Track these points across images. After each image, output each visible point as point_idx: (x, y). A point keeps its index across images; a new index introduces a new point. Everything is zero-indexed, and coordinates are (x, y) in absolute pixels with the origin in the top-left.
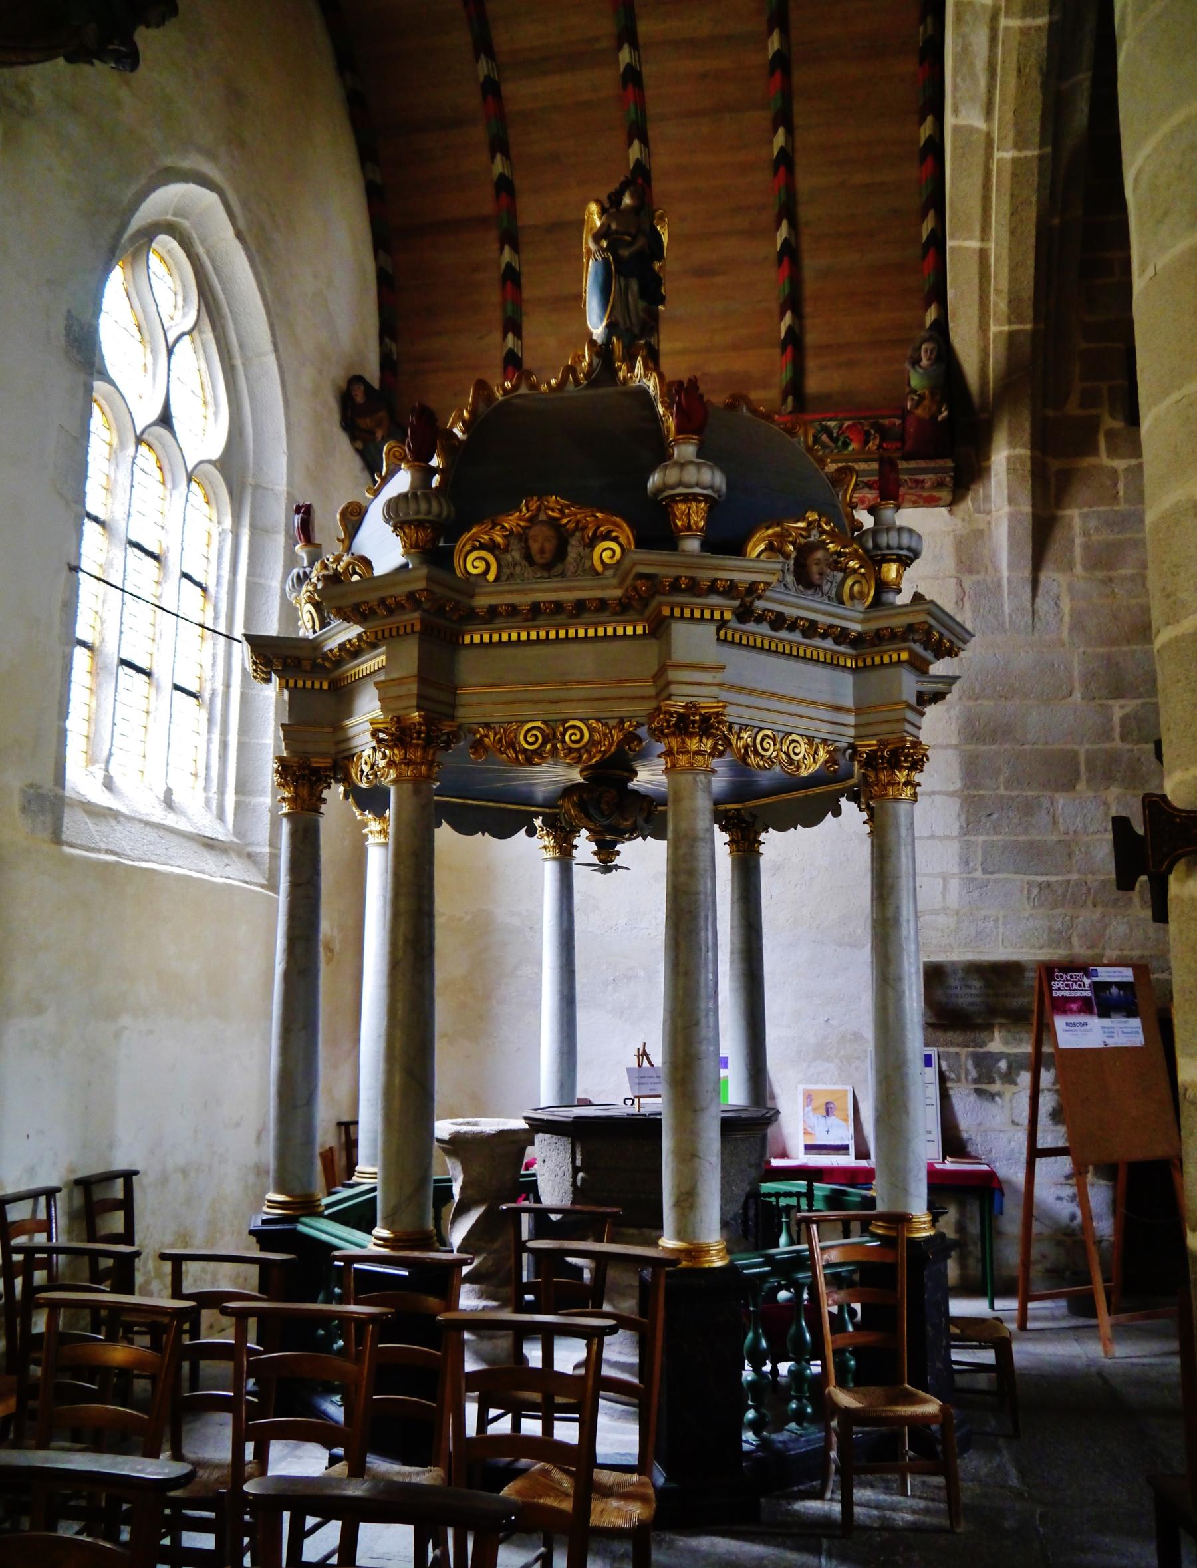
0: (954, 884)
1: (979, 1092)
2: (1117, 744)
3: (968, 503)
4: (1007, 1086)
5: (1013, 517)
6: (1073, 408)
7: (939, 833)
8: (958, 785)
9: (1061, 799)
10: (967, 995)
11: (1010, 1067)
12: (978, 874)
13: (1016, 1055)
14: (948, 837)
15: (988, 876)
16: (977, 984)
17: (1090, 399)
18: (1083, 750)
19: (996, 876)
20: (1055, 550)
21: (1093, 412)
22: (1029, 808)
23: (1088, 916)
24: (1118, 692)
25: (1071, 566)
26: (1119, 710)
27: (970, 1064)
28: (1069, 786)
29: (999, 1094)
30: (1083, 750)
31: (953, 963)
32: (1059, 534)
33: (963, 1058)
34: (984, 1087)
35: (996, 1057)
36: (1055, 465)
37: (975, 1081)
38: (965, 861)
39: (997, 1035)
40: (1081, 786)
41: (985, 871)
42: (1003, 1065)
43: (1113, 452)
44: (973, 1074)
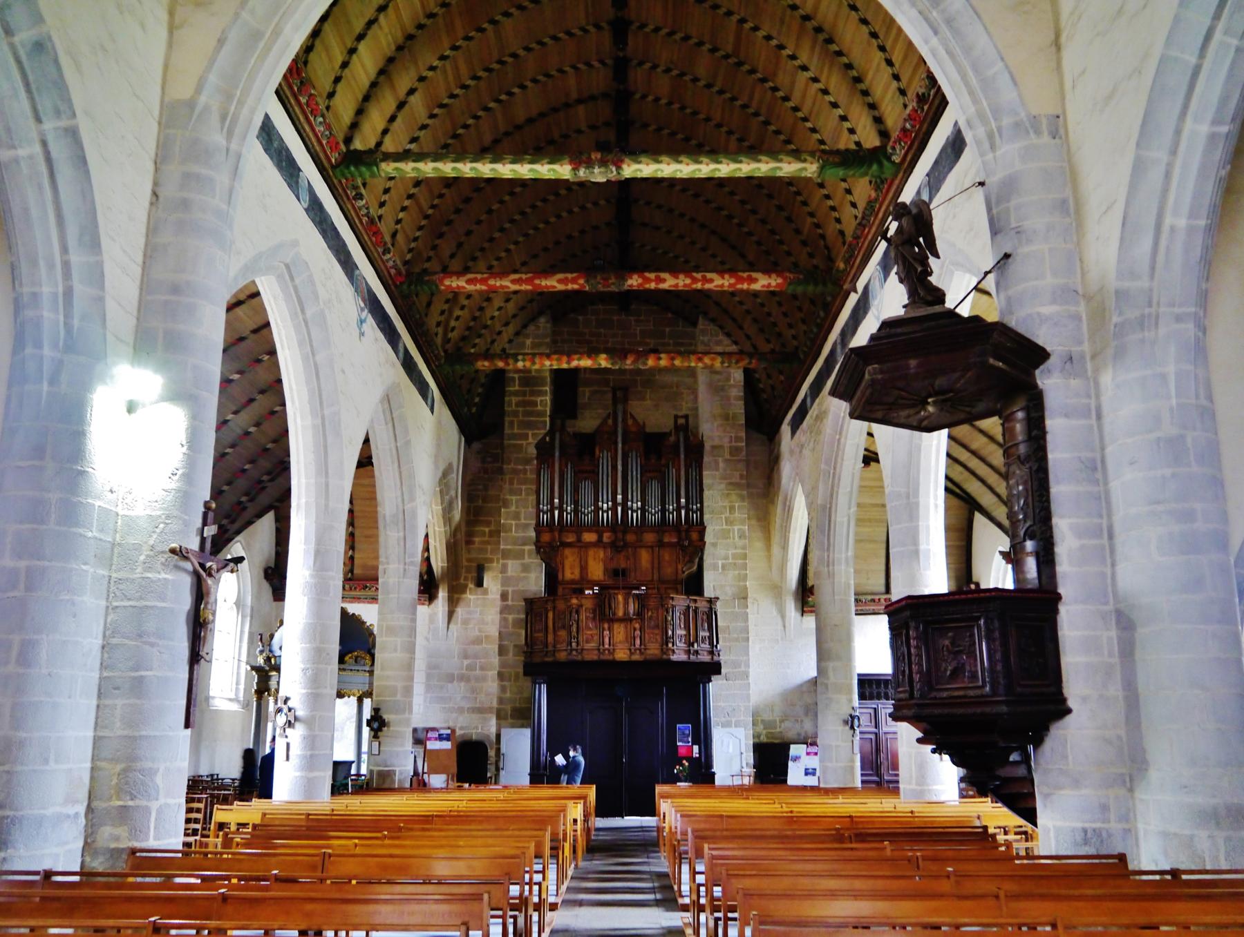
2: (464, 671)
3: (433, 605)
5: (443, 611)
6: (462, 581)
9: (450, 685)
17: (466, 578)
18: (456, 673)
20: (454, 619)
22: (442, 687)
23: (454, 715)
24: (466, 657)
25: (457, 624)
26: (466, 662)
30: (456, 673)
32: (455, 615)
36: (456, 596)
38: (425, 701)
43: (470, 594)
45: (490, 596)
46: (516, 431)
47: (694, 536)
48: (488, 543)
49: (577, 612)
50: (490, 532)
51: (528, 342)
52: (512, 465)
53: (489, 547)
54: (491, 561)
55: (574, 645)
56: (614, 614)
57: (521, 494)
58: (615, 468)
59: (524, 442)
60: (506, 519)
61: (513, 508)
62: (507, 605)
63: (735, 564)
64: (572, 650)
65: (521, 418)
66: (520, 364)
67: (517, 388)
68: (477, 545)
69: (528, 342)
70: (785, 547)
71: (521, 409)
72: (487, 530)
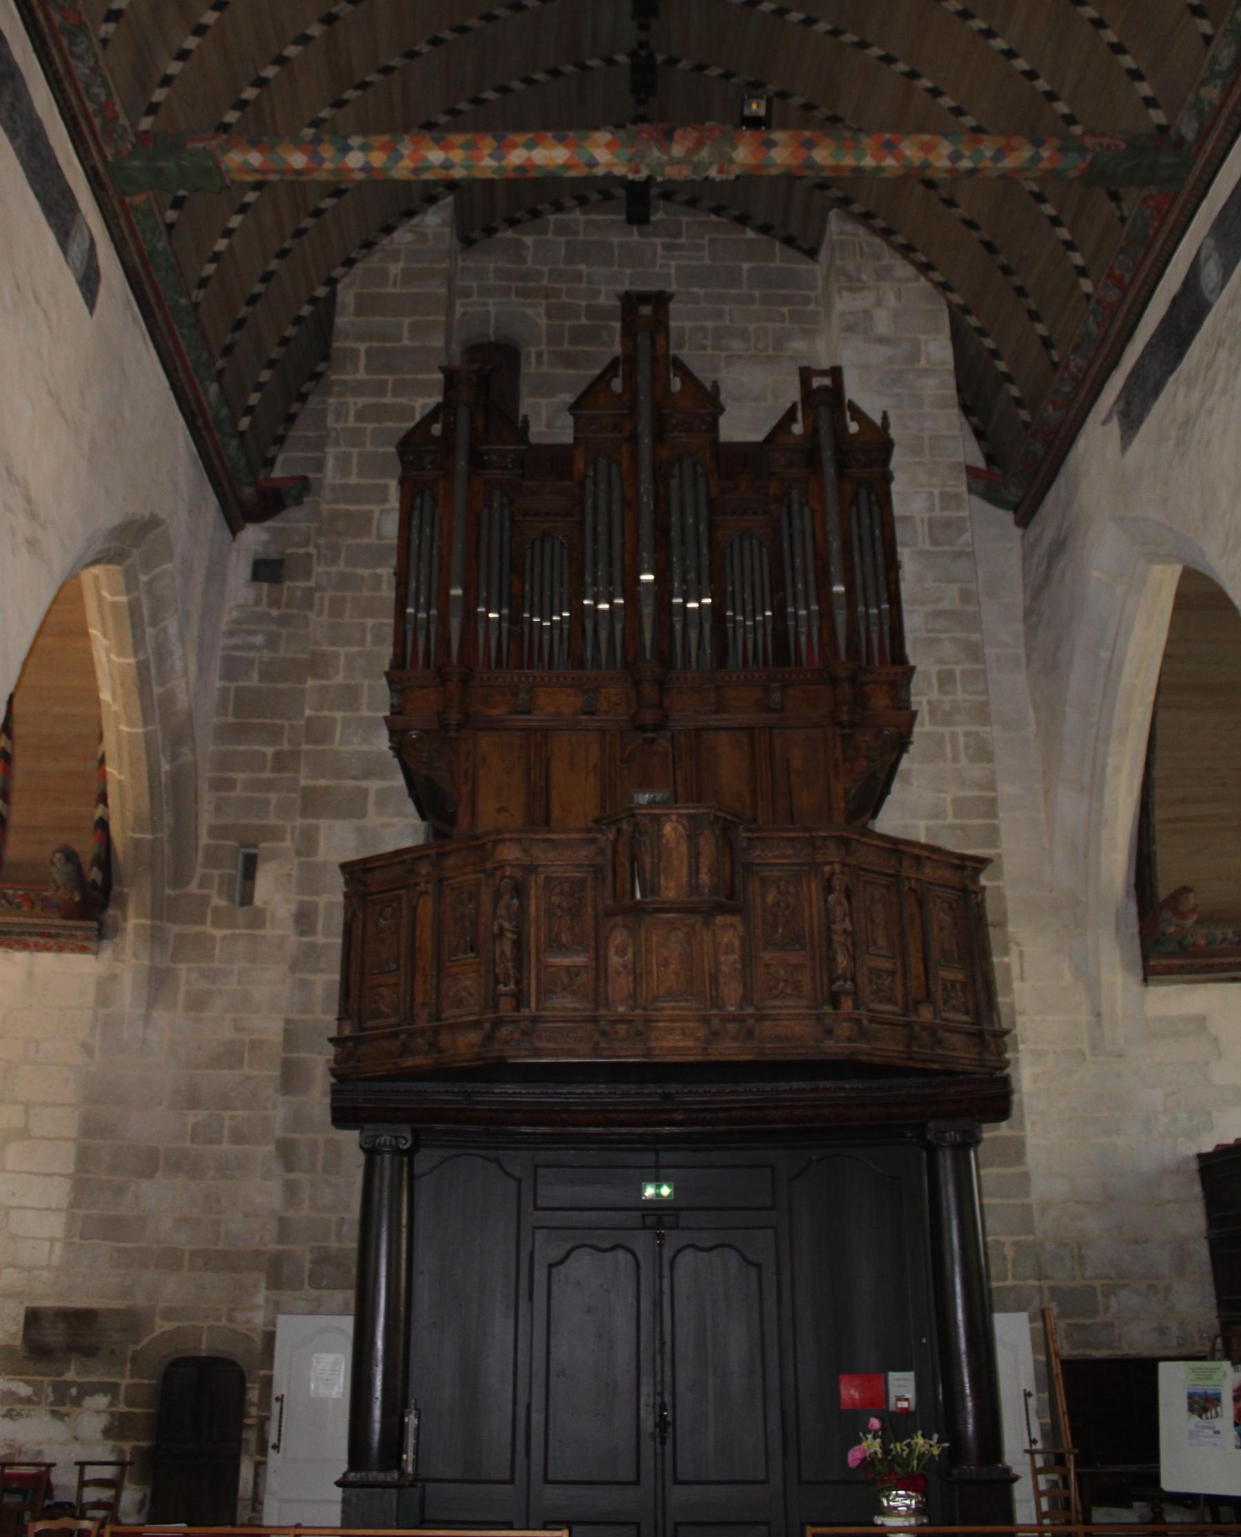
0: (58, 1247)
1: (54, 1413)
4: (75, 1408)
7: (54, 1205)
8: (72, 1169)
10: (54, 1335)
11: (79, 1393)
12: (77, 1240)
13: (84, 1383)
14: (59, 1210)
15: (83, 1242)
16: (62, 1326)
19: (89, 1241)
21: (206, 892)
27: (49, 1391)
28: (149, 1173)
29: (68, 1415)
31: (47, 1309)
33: (46, 1384)
34: (57, 1408)
35: (69, 1384)
37: (52, 1404)
39: (73, 1366)
40: (158, 1174)
41: (82, 1237)
42: (74, 1391)
44: (51, 1398)
45: (269, 932)
46: (354, 480)
47: (880, 701)
48: (269, 785)
49: (519, 890)
50: (278, 755)
51: (395, 268)
52: (341, 567)
53: (273, 797)
54: (275, 834)
55: (506, 1005)
56: (651, 888)
57: (361, 642)
58: (630, 505)
59: (376, 508)
60: (320, 707)
61: (339, 679)
62: (313, 946)
63: (962, 828)
64: (498, 1023)
65: (369, 448)
66: (355, 160)
67: (362, 375)
68: (239, 792)
69: (395, 268)
70: (1094, 787)
71: (370, 426)
72: (269, 750)
